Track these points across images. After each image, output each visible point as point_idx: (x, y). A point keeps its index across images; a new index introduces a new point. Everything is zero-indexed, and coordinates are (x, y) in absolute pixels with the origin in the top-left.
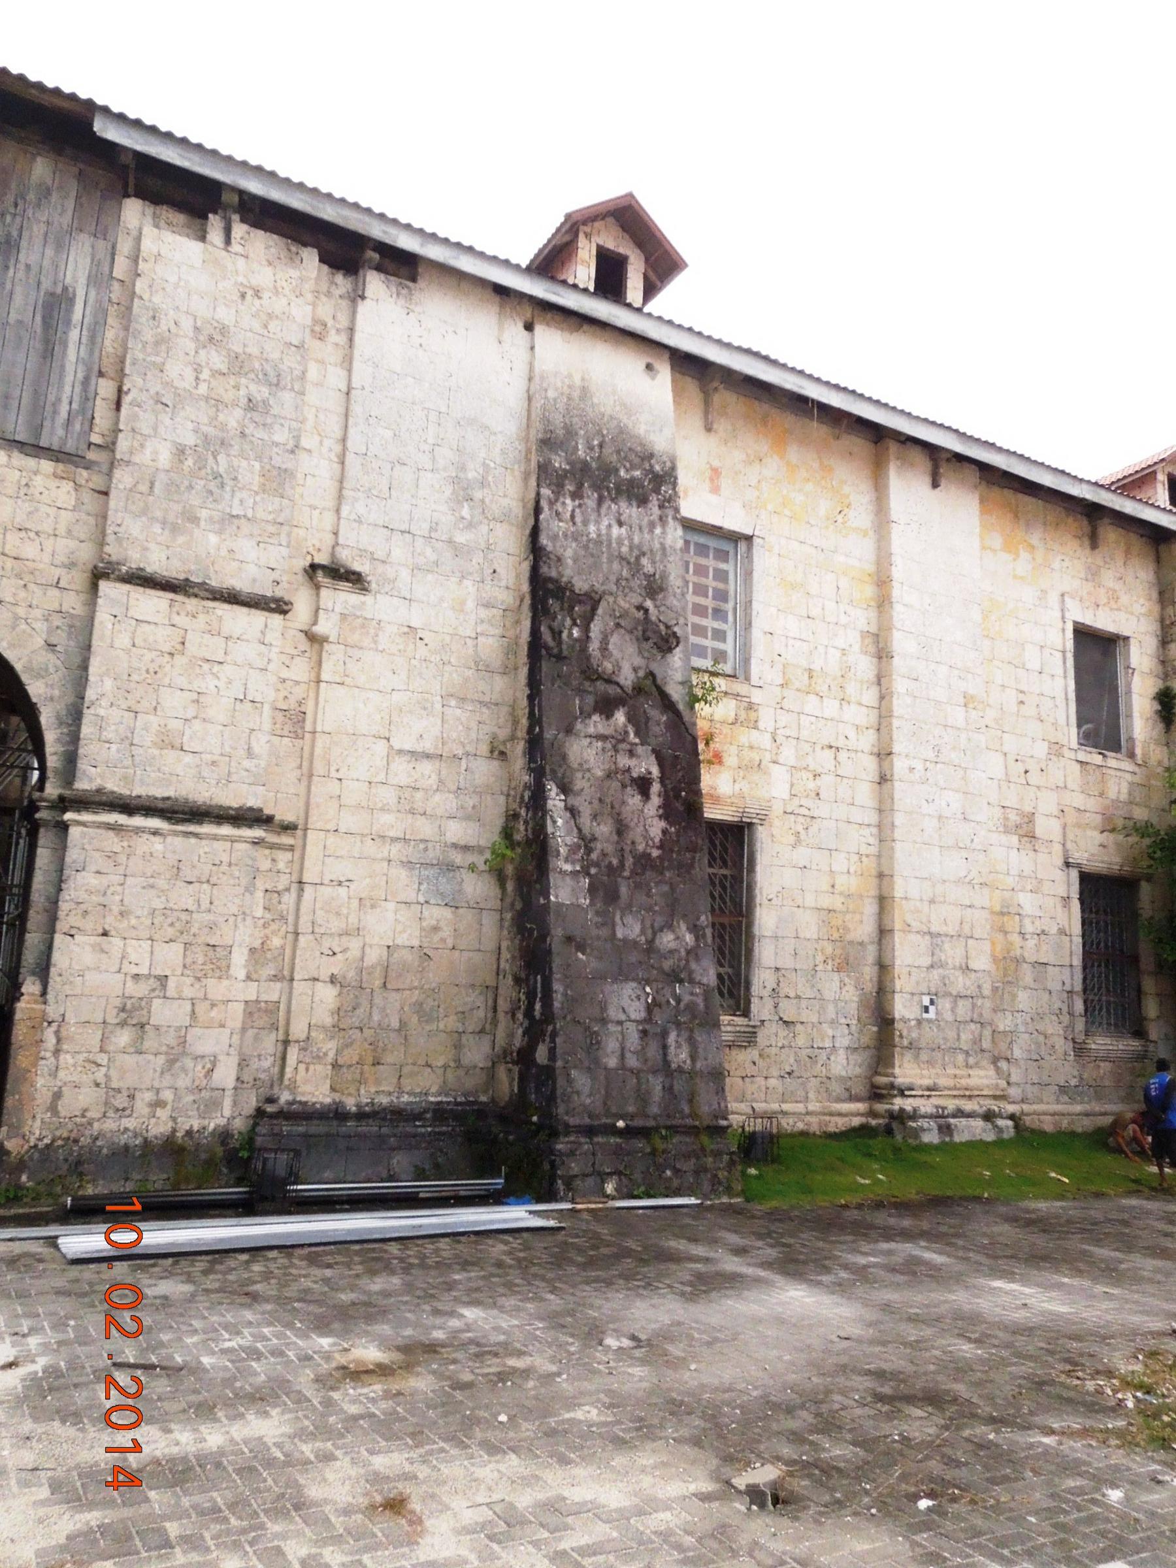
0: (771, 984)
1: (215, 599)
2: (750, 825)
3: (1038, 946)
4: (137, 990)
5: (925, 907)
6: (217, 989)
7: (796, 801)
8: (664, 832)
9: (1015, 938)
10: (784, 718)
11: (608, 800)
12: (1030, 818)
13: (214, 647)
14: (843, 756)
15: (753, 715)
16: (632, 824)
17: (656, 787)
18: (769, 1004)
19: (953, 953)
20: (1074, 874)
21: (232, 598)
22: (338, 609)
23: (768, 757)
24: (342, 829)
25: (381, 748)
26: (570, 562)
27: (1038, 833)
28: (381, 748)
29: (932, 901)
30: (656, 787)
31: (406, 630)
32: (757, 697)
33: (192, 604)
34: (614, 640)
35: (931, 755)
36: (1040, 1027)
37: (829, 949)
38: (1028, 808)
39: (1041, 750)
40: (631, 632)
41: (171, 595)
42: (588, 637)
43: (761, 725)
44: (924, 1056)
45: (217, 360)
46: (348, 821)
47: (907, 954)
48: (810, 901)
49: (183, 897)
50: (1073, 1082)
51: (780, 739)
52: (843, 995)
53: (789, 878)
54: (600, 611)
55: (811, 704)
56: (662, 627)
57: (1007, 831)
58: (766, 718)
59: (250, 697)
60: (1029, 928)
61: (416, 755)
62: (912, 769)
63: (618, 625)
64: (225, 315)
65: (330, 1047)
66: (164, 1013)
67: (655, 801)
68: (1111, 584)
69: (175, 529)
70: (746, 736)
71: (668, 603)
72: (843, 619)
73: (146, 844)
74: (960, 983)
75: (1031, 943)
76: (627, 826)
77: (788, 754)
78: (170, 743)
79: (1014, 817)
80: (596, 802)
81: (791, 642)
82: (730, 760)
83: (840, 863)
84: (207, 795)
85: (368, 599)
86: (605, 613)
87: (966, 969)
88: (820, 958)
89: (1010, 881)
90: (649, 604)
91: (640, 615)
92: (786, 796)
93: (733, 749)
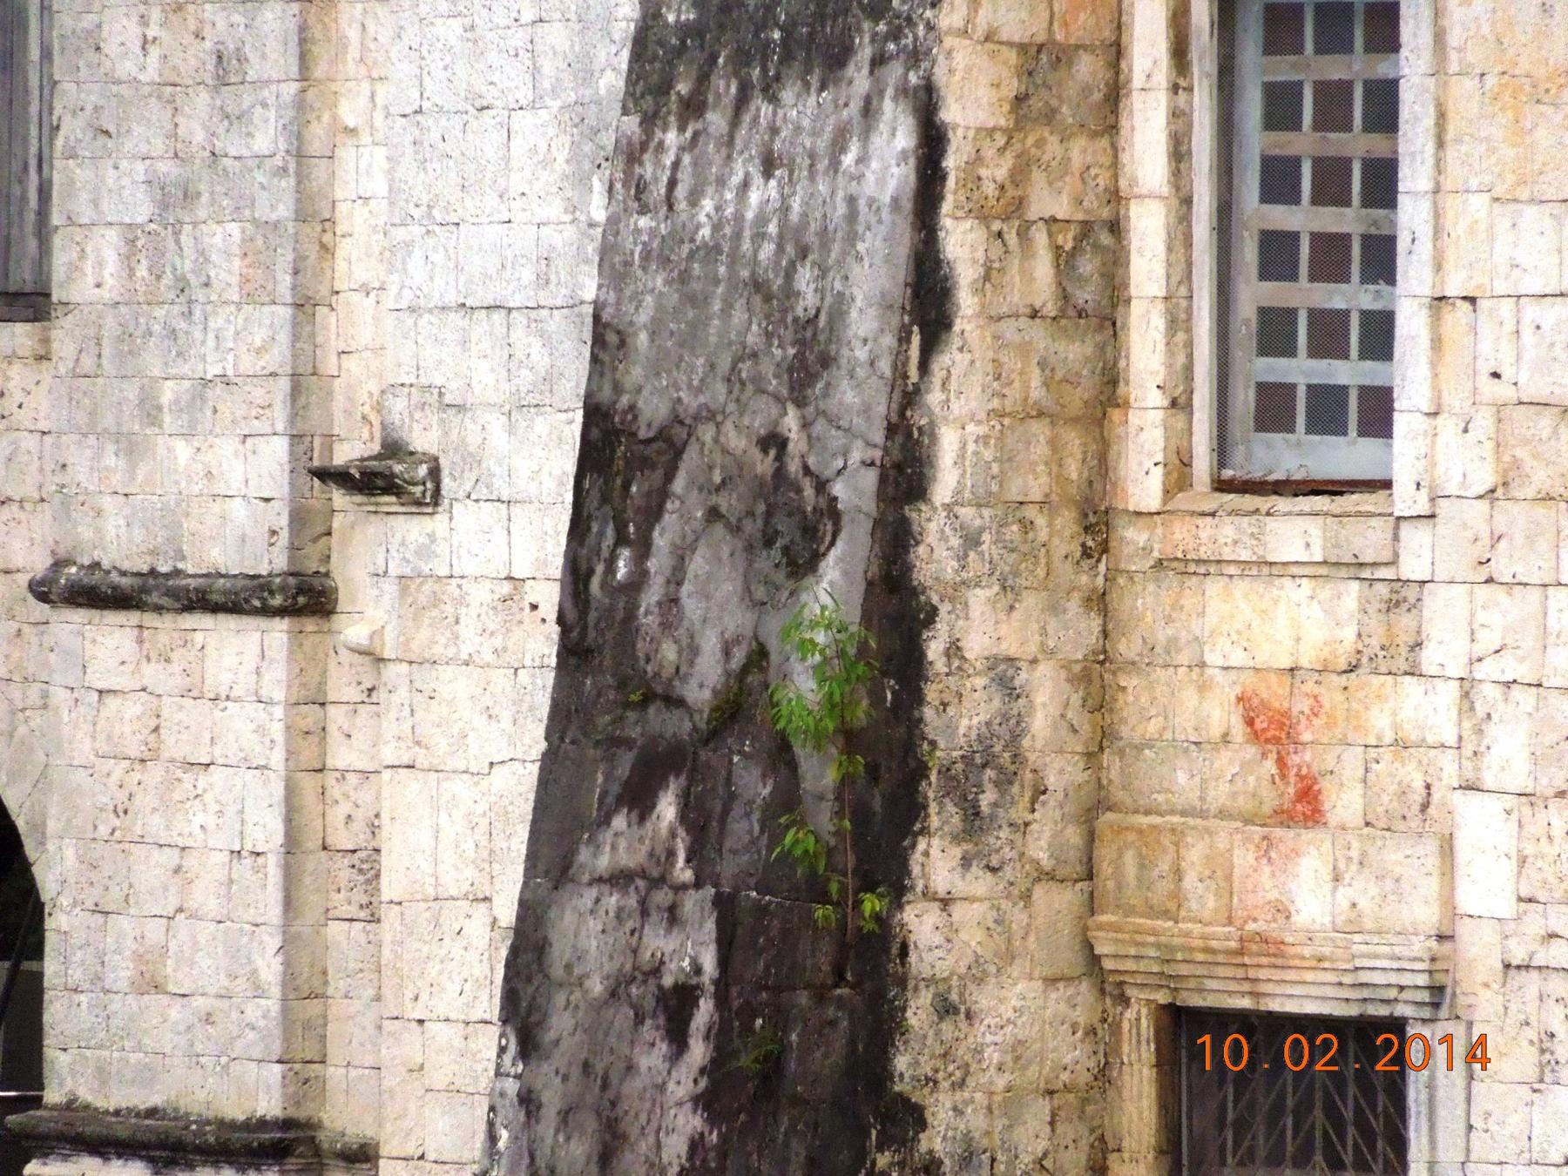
1: (189, 608)
2: (1397, 1026)
7: (1535, 924)
8: (696, 1144)
11: (599, 1067)
15: (1405, 621)
16: (634, 1132)
17: (704, 1012)
22: (394, 570)
23: (1449, 770)
24: (431, 1156)
26: (643, 337)
30: (704, 1012)
31: (506, 588)
33: (166, 627)
34: (698, 564)
40: (736, 530)
41: (134, 617)
42: (645, 574)
43: (1430, 658)
51: (1488, 694)
54: (678, 485)
56: (809, 492)
59: (249, 847)
63: (714, 514)
67: (698, 1051)
69: (132, 449)
71: (831, 405)
76: (624, 1137)
77: (1510, 754)
80: (576, 1073)
81: (1531, 311)
82: (1344, 802)
84: (201, 1095)
85: (437, 524)
86: (687, 488)
90: (791, 423)
91: (764, 465)
92: (1506, 907)
93: (1352, 762)
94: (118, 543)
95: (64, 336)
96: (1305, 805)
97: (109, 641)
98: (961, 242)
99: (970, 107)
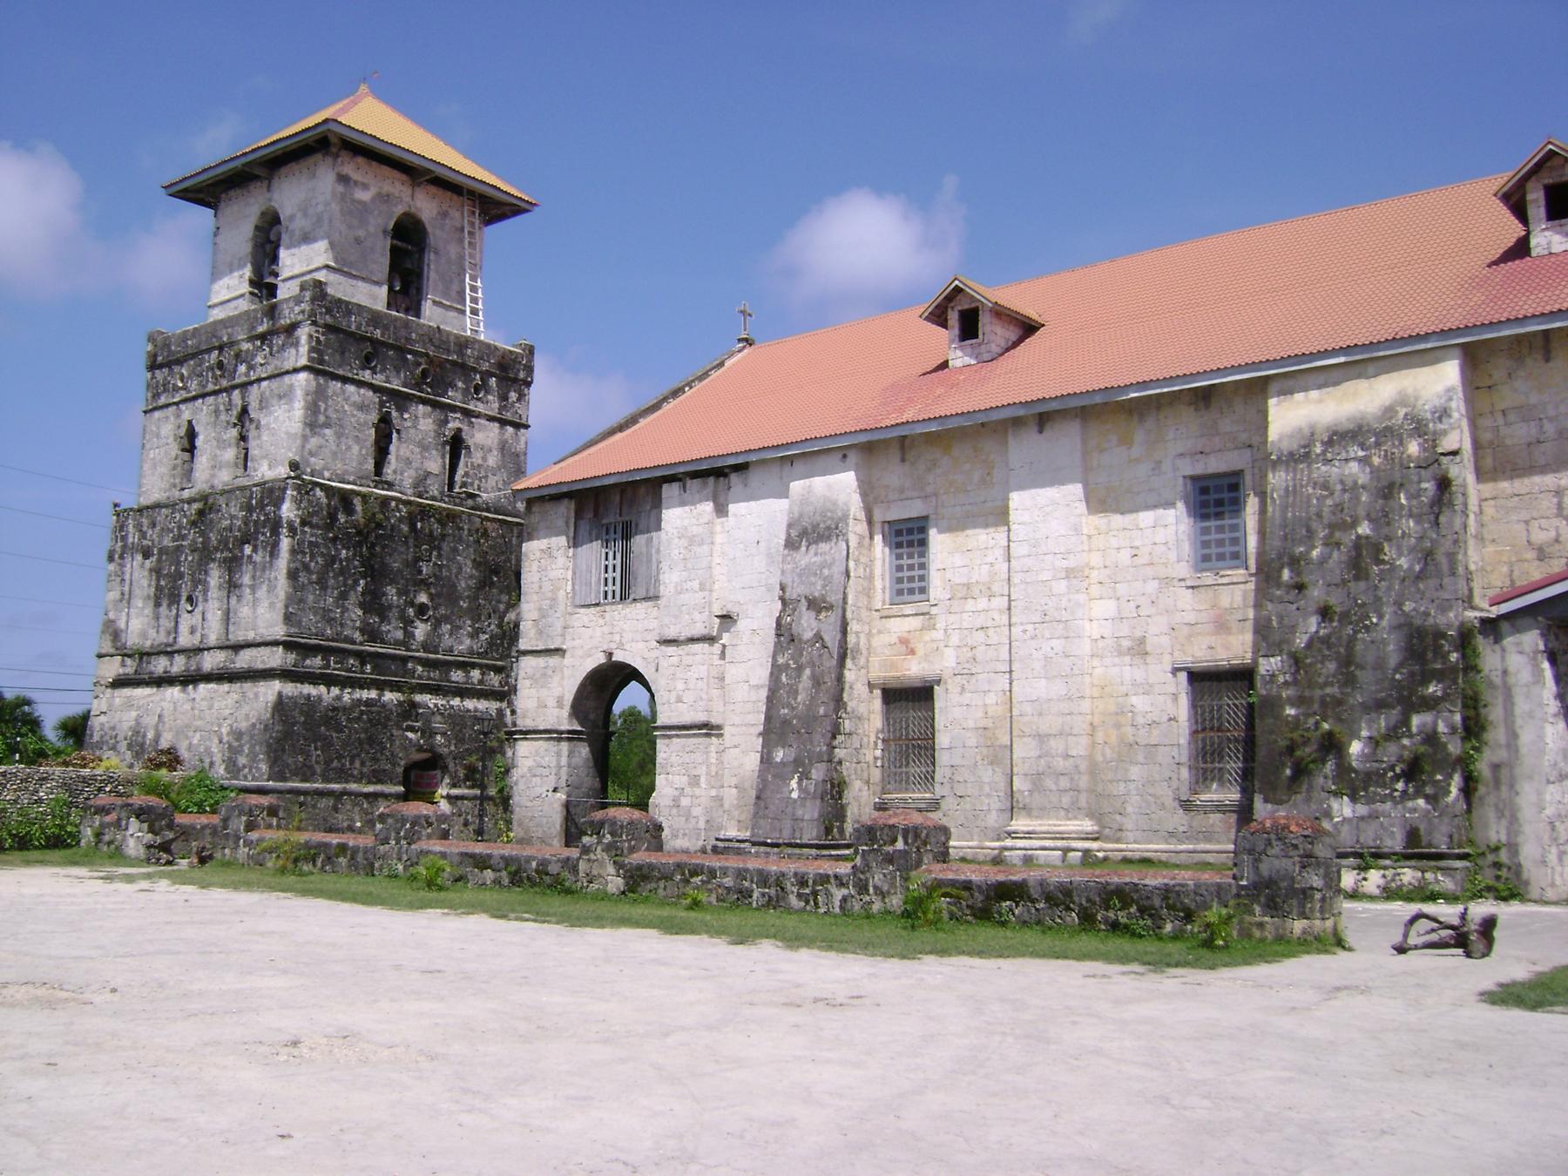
0: (948, 772)
3: (1150, 732)
4: (676, 793)
5: (1036, 719)
6: (697, 791)
9: (1129, 730)
10: (952, 618)
12: (1142, 641)
13: (688, 660)
14: (991, 632)
18: (947, 786)
19: (1056, 745)
20: (1183, 676)
21: (692, 640)
25: (746, 687)
27: (1148, 649)
28: (746, 687)
29: (1040, 714)
32: (934, 611)
35: (1037, 618)
36: (1151, 791)
37: (985, 751)
38: (1138, 634)
39: (1152, 586)
44: (1035, 813)
45: (684, 542)
46: (737, 720)
47: (1024, 751)
48: (971, 724)
49: (687, 758)
50: (1182, 829)
52: (992, 777)
53: (957, 713)
55: (970, 605)
57: (1120, 654)
58: (940, 625)
60: (1140, 720)
61: (758, 687)
62: (1025, 631)
64: (686, 522)
65: (736, 813)
66: (685, 802)
68: (1228, 429)
70: (928, 636)
72: (992, 543)
73: (675, 740)
74: (1060, 764)
75: (1142, 731)
78: (679, 700)
79: (1126, 643)
82: (920, 652)
83: (991, 699)
87: (1067, 756)
88: (979, 758)
89: (1124, 689)
94: (671, 633)
95: (661, 602)
96: (912, 652)
97: (671, 650)
98: (852, 564)
99: (853, 544)
